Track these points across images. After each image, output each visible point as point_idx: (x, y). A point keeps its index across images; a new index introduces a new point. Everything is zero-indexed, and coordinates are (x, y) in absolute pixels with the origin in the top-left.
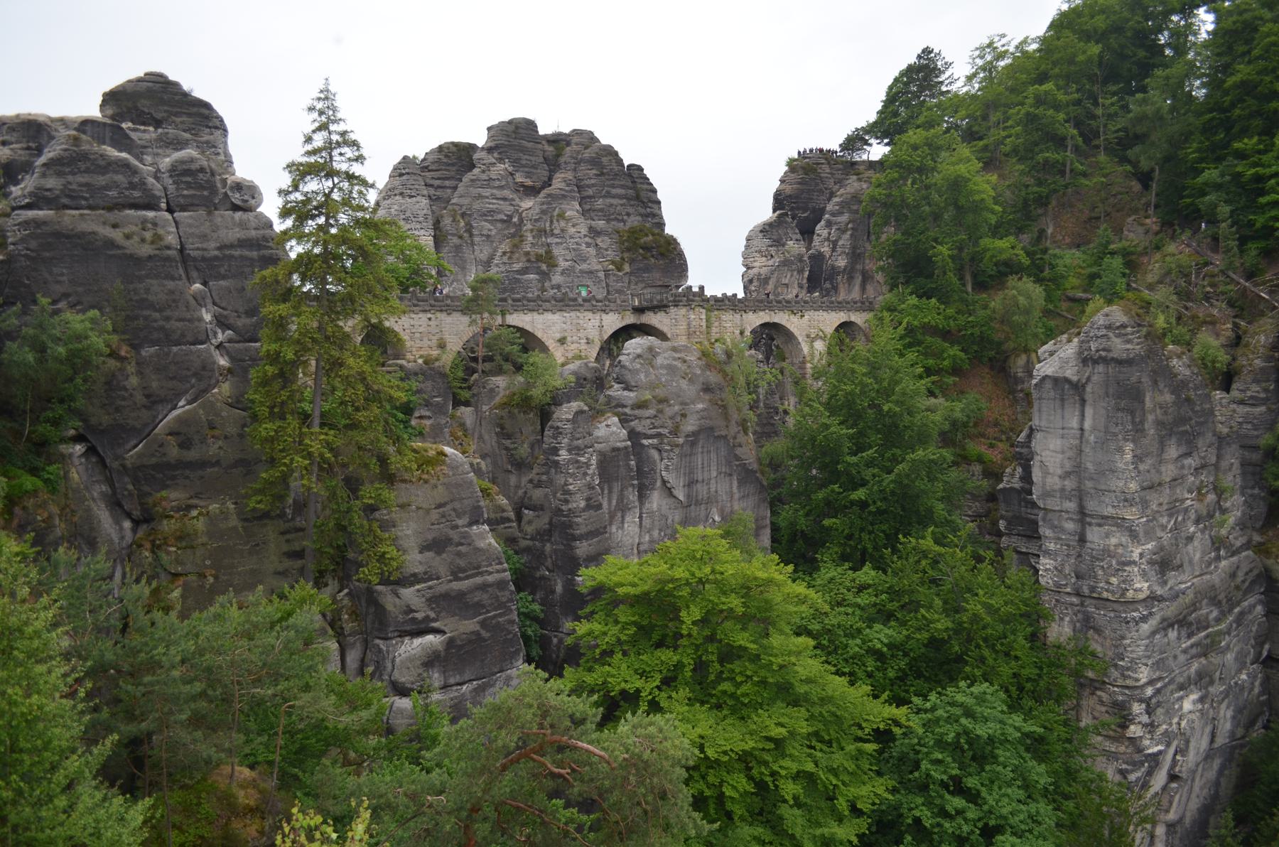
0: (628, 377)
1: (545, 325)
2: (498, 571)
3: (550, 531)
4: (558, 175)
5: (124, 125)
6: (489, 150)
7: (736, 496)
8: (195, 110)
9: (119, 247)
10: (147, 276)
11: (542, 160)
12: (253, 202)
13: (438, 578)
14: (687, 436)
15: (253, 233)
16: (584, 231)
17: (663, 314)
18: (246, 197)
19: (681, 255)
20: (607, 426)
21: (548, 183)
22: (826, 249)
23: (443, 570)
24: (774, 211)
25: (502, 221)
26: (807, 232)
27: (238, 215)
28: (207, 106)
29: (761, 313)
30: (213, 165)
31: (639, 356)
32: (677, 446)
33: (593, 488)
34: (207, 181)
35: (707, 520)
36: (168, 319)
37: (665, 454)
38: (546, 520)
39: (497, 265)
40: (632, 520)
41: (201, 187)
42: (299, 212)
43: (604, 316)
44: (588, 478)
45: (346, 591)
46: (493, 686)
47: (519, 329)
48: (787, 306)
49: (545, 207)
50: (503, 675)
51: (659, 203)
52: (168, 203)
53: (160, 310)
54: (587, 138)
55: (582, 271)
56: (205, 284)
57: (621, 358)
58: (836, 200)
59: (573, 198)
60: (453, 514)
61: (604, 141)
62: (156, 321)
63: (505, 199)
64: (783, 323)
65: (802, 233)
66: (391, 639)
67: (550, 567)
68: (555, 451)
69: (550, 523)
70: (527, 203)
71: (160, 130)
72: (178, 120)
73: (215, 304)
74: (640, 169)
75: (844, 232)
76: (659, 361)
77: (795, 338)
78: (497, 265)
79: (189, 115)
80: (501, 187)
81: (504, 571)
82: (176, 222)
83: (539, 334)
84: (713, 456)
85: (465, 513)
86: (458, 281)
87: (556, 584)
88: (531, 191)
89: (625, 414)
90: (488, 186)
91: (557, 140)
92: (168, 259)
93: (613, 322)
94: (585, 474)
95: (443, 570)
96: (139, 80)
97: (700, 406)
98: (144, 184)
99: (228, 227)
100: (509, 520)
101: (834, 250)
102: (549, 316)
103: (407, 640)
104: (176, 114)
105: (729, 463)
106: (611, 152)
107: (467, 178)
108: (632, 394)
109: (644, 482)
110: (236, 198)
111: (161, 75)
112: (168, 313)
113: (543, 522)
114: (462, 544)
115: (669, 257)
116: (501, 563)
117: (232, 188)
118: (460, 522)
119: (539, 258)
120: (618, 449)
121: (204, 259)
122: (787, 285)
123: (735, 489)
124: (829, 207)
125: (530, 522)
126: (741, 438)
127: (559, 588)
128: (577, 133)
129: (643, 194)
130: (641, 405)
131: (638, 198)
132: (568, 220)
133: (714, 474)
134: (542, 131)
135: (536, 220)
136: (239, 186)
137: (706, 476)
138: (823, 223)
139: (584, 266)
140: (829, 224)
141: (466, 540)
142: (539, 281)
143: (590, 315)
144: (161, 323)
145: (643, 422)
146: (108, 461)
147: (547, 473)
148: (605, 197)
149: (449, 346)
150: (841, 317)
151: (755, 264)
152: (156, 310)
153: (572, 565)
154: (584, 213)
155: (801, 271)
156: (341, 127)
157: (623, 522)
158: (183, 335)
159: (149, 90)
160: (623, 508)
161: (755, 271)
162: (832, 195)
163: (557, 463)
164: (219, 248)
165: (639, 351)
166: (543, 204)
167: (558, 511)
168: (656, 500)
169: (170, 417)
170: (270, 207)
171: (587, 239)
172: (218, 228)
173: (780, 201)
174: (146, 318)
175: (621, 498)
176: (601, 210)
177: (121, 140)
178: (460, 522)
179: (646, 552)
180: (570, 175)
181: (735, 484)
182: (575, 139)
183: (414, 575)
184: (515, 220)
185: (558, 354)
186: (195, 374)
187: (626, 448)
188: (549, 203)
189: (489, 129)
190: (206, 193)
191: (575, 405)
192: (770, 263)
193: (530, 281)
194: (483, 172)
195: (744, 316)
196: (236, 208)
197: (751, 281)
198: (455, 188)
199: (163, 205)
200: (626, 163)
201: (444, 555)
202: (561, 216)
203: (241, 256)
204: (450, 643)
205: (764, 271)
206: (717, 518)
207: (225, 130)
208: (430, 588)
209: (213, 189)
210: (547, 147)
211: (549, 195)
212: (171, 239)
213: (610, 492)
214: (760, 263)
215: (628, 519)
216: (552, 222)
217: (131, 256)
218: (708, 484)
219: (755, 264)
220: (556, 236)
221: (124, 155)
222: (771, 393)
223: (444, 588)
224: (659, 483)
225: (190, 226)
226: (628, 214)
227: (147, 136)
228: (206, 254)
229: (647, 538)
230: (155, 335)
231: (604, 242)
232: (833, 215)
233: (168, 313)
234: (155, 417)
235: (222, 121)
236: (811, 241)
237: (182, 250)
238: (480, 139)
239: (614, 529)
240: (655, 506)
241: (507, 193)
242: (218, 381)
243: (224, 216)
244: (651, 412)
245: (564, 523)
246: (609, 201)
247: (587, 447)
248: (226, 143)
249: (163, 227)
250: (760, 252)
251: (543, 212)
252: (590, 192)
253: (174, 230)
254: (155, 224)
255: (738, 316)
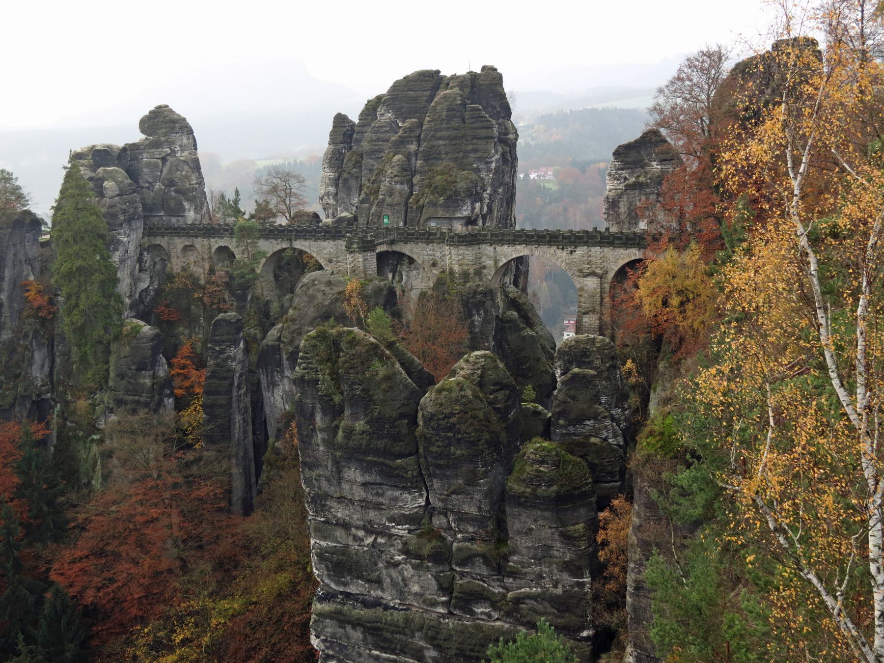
29: (518, 247)
72: (160, 132)
86: (345, 203)
195: (498, 248)
226: (447, 153)
247: (224, 341)
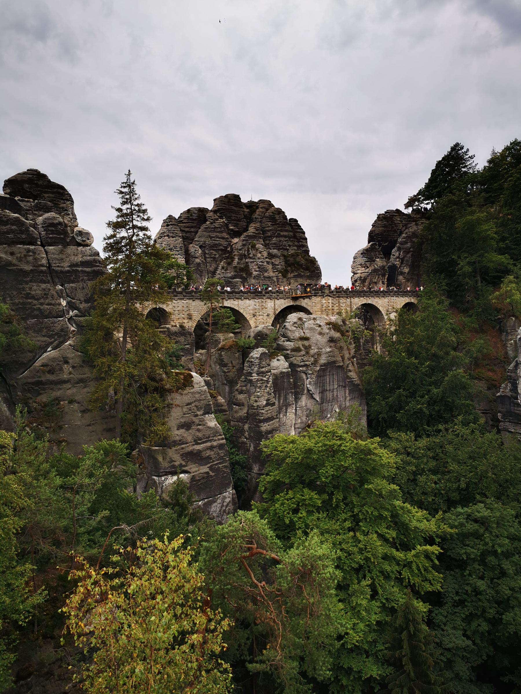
0: (289, 334)
1: (245, 306)
2: (219, 440)
3: (247, 417)
4: (251, 225)
5: (16, 198)
6: (214, 211)
7: (348, 399)
8: (55, 190)
9: (14, 265)
10: (31, 281)
11: (243, 217)
12: (88, 241)
13: (187, 443)
14: (321, 366)
15: (89, 258)
16: (265, 254)
17: (308, 300)
18: (84, 239)
19: (318, 269)
20: (278, 360)
21: (246, 230)
22: (398, 263)
23: (190, 439)
24: (369, 243)
25: (221, 250)
26: (387, 254)
27: (80, 248)
28: (62, 188)
29: (362, 299)
30: (66, 221)
31: (295, 323)
32: (316, 371)
33: (270, 394)
34: (63, 230)
35: (332, 412)
36: (42, 304)
37: (309, 376)
38: (245, 411)
39: (219, 274)
40: (291, 411)
41: (59, 233)
42: (114, 247)
43: (277, 302)
44: (268, 389)
45: (137, 450)
46: (215, 502)
47: (232, 309)
48: (378, 294)
49: (244, 242)
50: (221, 496)
51: (306, 239)
52: (41, 242)
53: (38, 299)
54: (268, 204)
55: (264, 277)
56: (62, 286)
57: (285, 324)
58: (404, 235)
59: (260, 238)
60: (195, 408)
61: (276, 206)
62: (35, 305)
63: (223, 238)
64: (374, 304)
65: (384, 254)
66: (161, 476)
67: (247, 436)
68: (250, 374)
69: (247, 413)
70: (236, 240)
71: (36, 201)
72: (46, 195)
73: (68, 296)
74: (296, 221)
75: (408, 253)
76: (306, 325)
77: (380, 312)
78: (219, 274)
79: (53, 193)
80: (221, 232)
81: (222, 439)
82: (46, 252)
83: (242, 311)
84: (335, 377)
85: (201, 408)
87: (250, 446)
88: (237, 234)
89: (288, 354)
90: (214, 231)
91: (252, 205)
92: (42, 272)
93: (282, 304)
94: (266, 386)
95: (190, 439)
96: (24, 173)
97: (328, 350)
98: (28, 231)
99: (75, 255)
100: (225, 411)
101: (402, 263)
102: (247, 301)
103: (169, 477)
104: (46, 192)
105: (344, 380)
106: (280, 212)
107: (204, 226)
108: (292, 344)
109: (298, 391)
110: (79, 239)
111: (36, 171)
112: (42, 301)
113: (243, 412)
114: (200, 425)
115: (312, 269)
116: (221, 435)
117: (76, 234)
118: (199, 413)
119: (242, 270)
120: (284, 372)
121: (62, 272)
122: (376, 283)
123: (347, 395)
124: (400, 240)
125: (236, 412)
126: (350, 367)
127: (252, 449)
128: (261, 201)
129: (297, 235)
130: (297, 350)
131: (295, 237)
132: (257, 250)
133: (336, 386)
134: (245, 199)
135: (240, 250)
136: (81, 233)
137: (331, 388)
138: (396, 248)
139: (266, 274)
140: (399, 249)
141: (202, 423)
142: (242, 282)
143: (269, 301)
144: (38, 306)
145: (298, 358)
146: (8, 380)
147: (246, 386)
148: (277, 237)
149: (194, 318)
150: (405, 300)
151: (359, 272)
152: (35, 299)
153: (259, 436)
154: (266, 246)
155: (383, 275)
156: (135, 203)
157: (286, 412)
158: (50, 312)
159: (29, 179)
160: (287, 405)
161: (358, 275)
162: (401, 233)
163: (251, 381)
164: (69, 266)
165: (295, 320)
166: (244, 241)
167: (251, 407)
168: (304, 401)
169: (43, 356)
170: (98, 245)
171: (267, 260)
172: (69, 255)
173: (372, 237)
174: (30, 303)
175: (286, 399)
176: (275, 244)
177: (15, 207)
178: (199, 413)
179: (298, 428)
180: (258, 225)
181: (347, 391)
182: (261, 205)
183: (175, 441)
184: (229, 249)
185: (252, 323)
186: (57, 334)
187: (288, 372)
188: (247, 240)
189: (215, 200)
190: (62, 236)
191: (261, 350)
192: (367, 270)
193: (237, 282)
194: (212, 223)
195: (352, 300)
196: (79, 245)
197: (356, 281)
198: (196, 232)
199: (39, 243)
200: (288, 218)
201: (190, 431)
202: (253, 247)
203: (82, 271)
204: (193, 479)
205: (363, 275)
206: (337, 410)
207: (73, 202)
208: (183, 448)
209: (65, 233)
210: (246, 210)
211: (247, 236)
212: (44, 262)
213: (279, 396)
214: (361, 271)
215: (288, 410)
216: (248, 251)
217: (21, 270)
218: (333, 392)
219: (359, 272)
220: (250, 258)
221: (16, 215)
222: (367, 341)
223: (191, 448)
224: (305, 392)
225: (54, 254)
227: (29, 204)
228: (62, 269)
229: (299, 421)
230: (36, 313)
231: (277, 261)
232: (401, 243)
233: (42, 301)
234: (35, 356)
235: (70, 196)
236: (389, 258)
237: (49, 267)
238: (210, 205)
239: (281, 416)
240: (304, 404)
241: (225, 235)
242: (70, 338)
243: (71, 249)
244: (303, 353)
245: (254, 413)
246: (278, 239)
247: (267, 372)
248: (73, 208)
249: (39, 254)
250: (361, 265)
251: (244, 245)
252: (269, 234)
253: (45, 256)
254: (34, 253)
255: (348, 300)
